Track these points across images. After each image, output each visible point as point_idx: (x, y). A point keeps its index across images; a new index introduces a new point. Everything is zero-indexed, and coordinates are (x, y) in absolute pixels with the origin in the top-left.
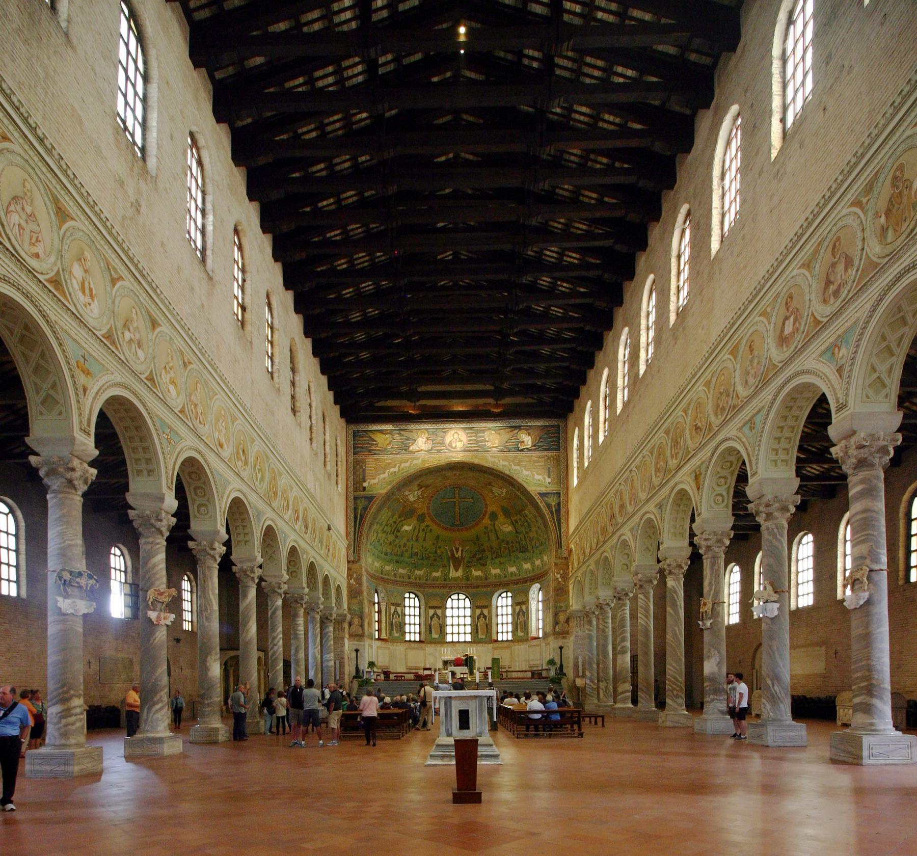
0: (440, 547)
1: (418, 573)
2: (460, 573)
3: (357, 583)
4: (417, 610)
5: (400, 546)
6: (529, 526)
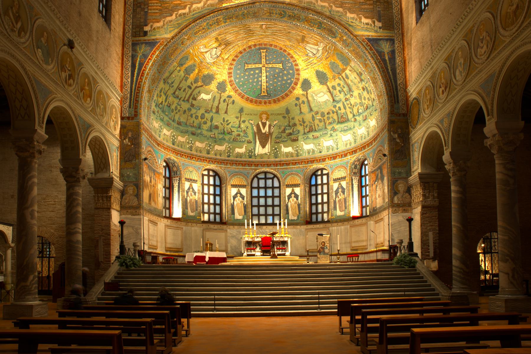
0: (244, 122)
3: (132, 144)
6: (350, 90)
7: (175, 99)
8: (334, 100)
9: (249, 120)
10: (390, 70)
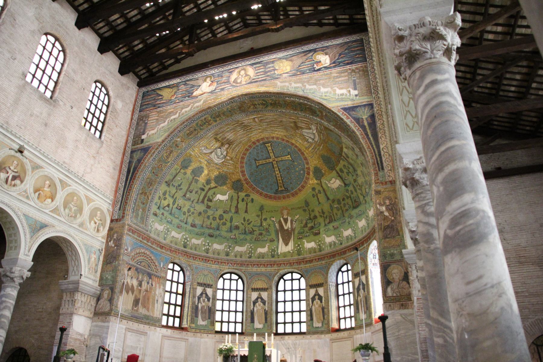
0: (265, 219)
1: (238, 249)
2: (290, 247)
4: (240, 294)
5: (214, 219)
7: (186, 202)
8: (345, 184)
9: (270, 217)
10: (370, 136)
